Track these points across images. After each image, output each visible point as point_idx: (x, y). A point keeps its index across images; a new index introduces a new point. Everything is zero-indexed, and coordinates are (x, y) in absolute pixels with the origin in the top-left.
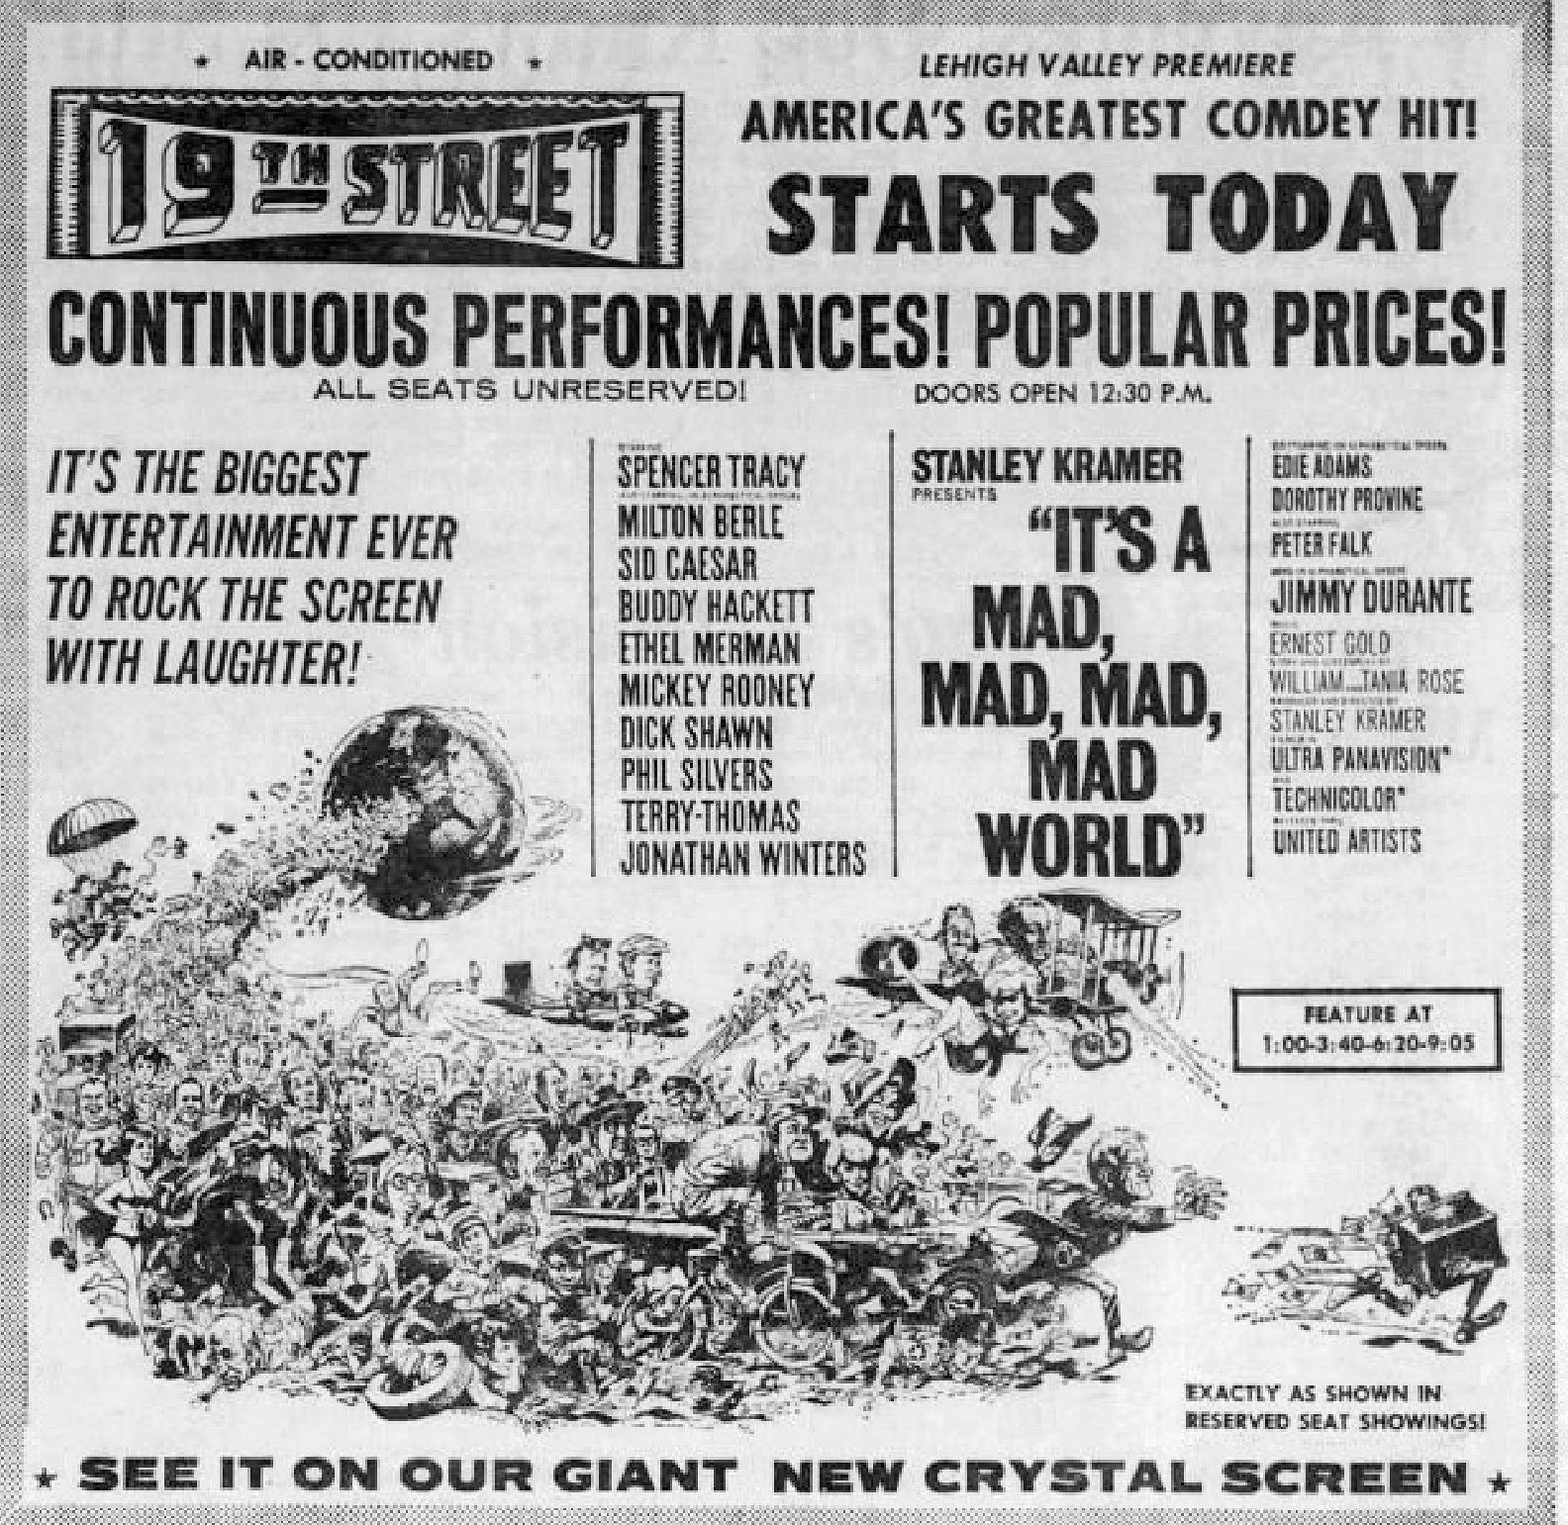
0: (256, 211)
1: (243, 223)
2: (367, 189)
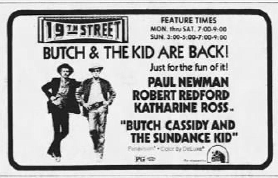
0: (67, 35)
1: (66, 37)
2: (83, 32)
